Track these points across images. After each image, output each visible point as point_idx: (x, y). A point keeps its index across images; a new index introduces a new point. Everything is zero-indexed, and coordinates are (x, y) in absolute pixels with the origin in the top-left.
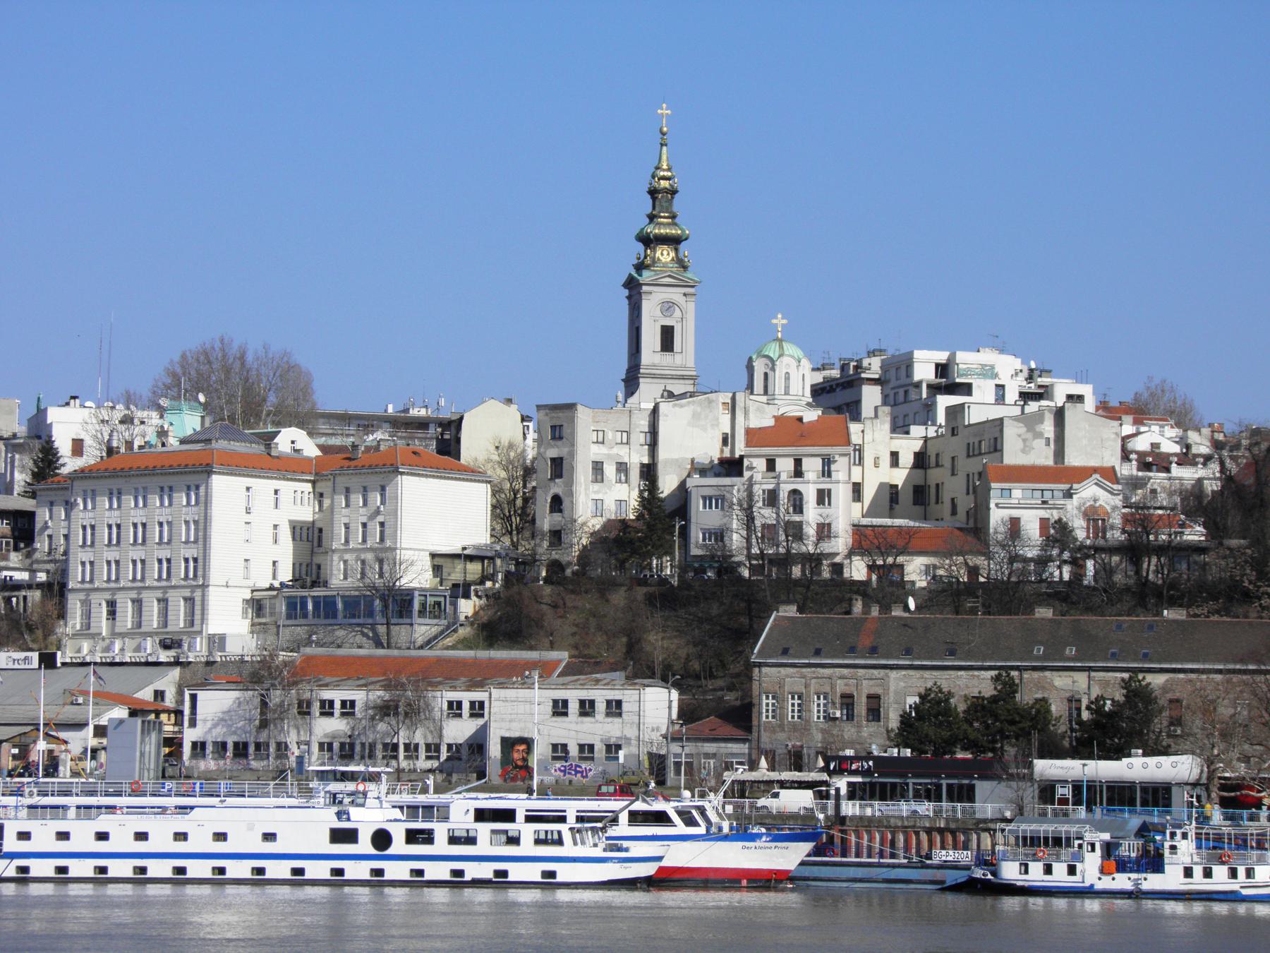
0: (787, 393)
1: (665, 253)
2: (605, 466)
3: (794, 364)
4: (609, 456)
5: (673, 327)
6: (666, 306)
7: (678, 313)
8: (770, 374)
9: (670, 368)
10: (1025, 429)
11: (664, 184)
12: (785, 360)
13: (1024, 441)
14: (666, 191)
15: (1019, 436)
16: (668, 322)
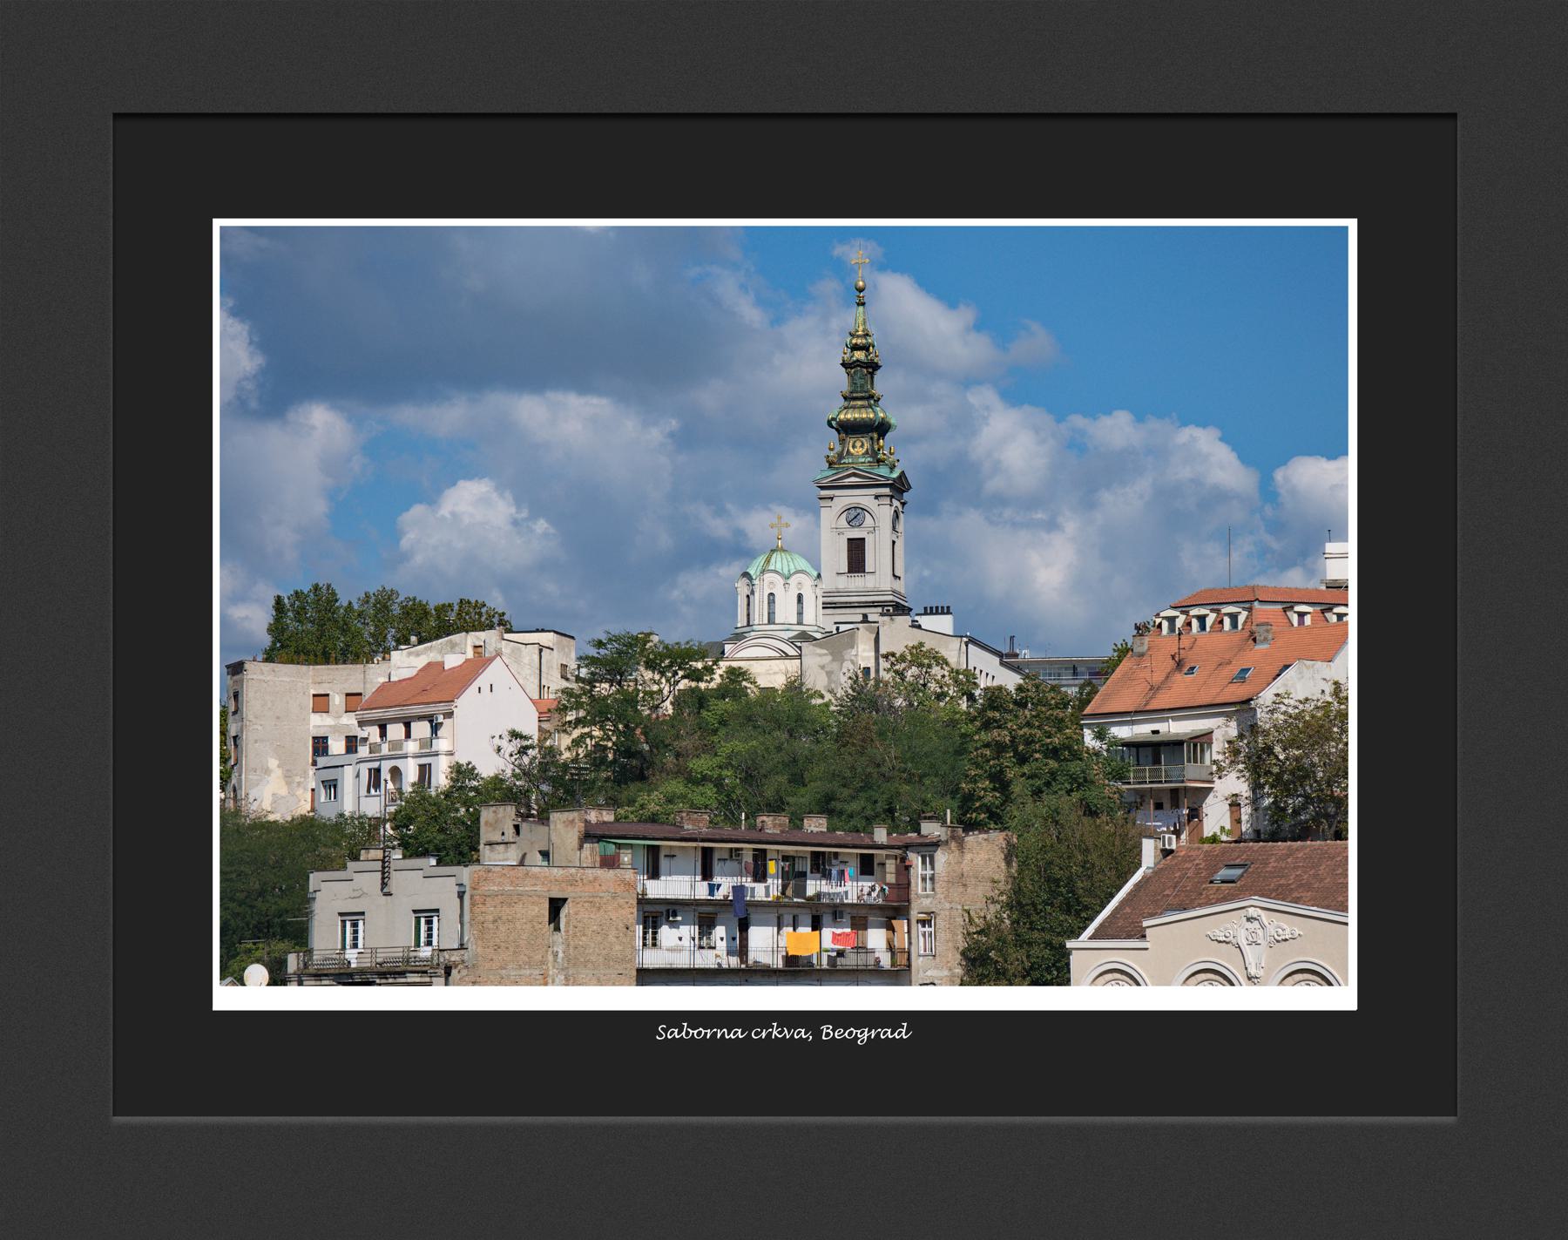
0: (771, 621)
1: (858, 444)
2: (330, 742)
3: (779, 580)
4: (335, 729)
5: (864, 539)
6: (853, 513)
7: (868, 521)
8: (751, 597)
9: (859, 593)
10: (829, 658)
11: (860, 355)
12: (768, 576)
13: (829, 674)
14: (858, 364)
15: (823, 667)
16: (856, 534)
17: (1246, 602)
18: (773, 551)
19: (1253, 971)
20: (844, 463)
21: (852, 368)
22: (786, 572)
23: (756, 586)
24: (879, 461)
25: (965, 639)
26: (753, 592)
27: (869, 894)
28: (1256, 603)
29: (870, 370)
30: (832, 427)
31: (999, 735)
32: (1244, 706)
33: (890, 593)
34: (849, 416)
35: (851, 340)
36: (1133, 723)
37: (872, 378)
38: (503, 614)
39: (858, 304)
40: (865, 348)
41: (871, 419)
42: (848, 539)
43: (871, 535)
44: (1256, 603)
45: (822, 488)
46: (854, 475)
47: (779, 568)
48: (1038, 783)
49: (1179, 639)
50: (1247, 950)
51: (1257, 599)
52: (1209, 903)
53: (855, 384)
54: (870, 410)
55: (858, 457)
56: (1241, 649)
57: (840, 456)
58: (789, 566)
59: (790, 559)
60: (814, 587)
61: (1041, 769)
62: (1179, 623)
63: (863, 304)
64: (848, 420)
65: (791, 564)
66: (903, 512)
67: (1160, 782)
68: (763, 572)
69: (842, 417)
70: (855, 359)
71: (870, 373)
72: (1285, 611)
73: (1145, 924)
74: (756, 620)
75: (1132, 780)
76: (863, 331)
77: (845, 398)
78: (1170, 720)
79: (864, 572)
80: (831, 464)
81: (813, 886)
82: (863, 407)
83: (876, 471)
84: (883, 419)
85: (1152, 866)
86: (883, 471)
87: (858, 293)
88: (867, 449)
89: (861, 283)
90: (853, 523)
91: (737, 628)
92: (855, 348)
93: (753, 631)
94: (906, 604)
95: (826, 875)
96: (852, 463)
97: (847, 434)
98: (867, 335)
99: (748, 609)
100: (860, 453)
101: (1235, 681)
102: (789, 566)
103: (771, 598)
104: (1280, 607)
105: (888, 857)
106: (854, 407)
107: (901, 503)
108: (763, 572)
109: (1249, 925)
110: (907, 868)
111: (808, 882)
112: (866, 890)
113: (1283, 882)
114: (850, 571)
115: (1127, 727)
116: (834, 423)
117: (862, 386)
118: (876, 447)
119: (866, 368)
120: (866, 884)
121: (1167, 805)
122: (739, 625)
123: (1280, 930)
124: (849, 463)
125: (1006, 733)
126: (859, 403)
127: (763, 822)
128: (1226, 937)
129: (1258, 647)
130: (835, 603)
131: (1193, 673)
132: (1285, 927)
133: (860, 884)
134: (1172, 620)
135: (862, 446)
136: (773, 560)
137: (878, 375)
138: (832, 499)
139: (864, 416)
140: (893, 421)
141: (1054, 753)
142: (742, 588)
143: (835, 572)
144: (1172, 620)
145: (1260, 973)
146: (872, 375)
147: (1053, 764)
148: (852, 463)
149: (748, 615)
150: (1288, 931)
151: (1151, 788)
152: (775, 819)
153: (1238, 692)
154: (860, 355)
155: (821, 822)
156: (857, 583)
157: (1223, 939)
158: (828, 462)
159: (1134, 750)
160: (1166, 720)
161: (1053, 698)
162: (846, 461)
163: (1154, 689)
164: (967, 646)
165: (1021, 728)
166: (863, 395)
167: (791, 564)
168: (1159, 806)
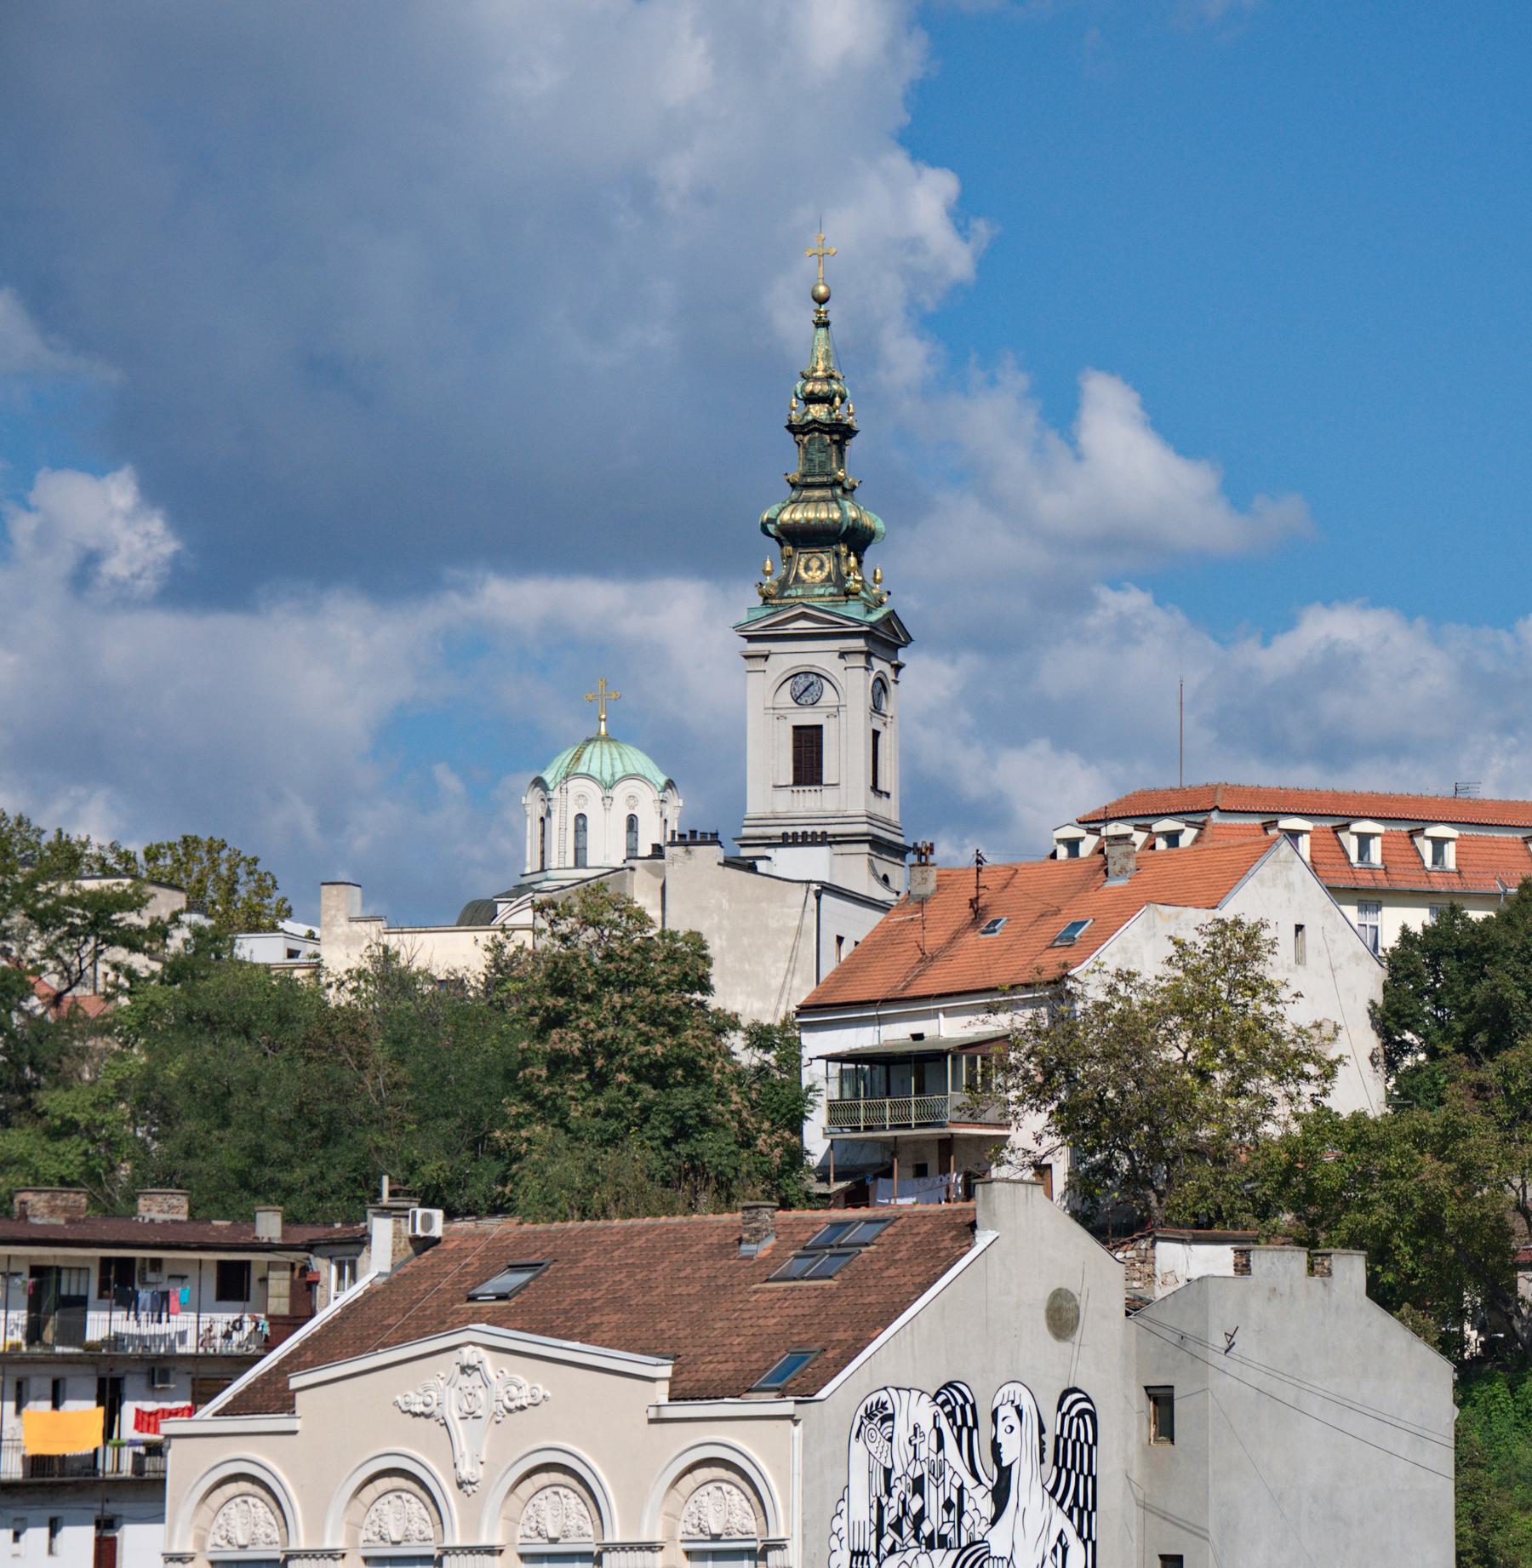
1: (815, 564)
3: (595, 791)
5: (820, 727)
6: (803, 682)
7: (829, 696)
8: (547, 821)
11: (818, 412)
12: (575, 785)
14: (813, 426)
16: (807, 718)
17: (1198, 812)
18: (589, 741)
19: (465, 1472)
20: (790, 597)
21: (805, 434)
22: (607, 777)
23: (553, 802)
24: (848, 593)
25: (815, 887)
26: (549, 813)
27: (227, 1336)
28: (1214, 815)
29: (836, 437)
30: (769, 535)
31: (562, 1039)
32: (1058, 989)
33: (865, 819)
34: (798, 516)
35: (803, 386)
36: (880, 1020)
37: (841, 452)
38: (255, 861)
39: (818, 325)
40: (827, 399)
41: (834, 522)
42: (796, 728)
43: (832, 720)
44: (1214, 815)
45: (751, 639)
46: (804, 616)
47: (594, 771)
48: (613, 1125)
49: (979, 870)
50: (458, 1428)
51: (1217, 807)
52: (403, 1339)
53: (811, 460)
54: (834, 505)
55: (814, 585)
56: (1084, 887)
57: (783, 584)
58: (613, 766)
59: (616, 755)
60: (658, 804)
61: (619, 1101)
62: (1085, 849)
63: (826, 325)
64: (796, 522)
65: (618, 763)
66: (896, 682)
67: (908, 1126)
68: (567, 777)
69: (786, 516)
70: (810, 418)
71: (835, 442)
72: (1335, 832)
73: (295, 1383)
74: (554, 861)
75: (913, 1122)
76: (825, 370)
77: (793, 485)
78: (941, 1015)
79: (819, 782)
80: (766, 598)
81: (100, 1325)
82: (824, 500)
83: (841, 611)
84: (855, 520)
85: (388, 1269)
86: (854, 610)
87: (816, 306)
88: (829, 573)
89: (822, 290)
90: (802, 701)
91: (523, 875)
92: (811, 399)
93: (547, 880)
94: (901, 840)
95: (127, 1301)
96: (803, 596)
97: (795, 546)
98: (832, 377)
99: (542, 842)
100: (817, 580)
101: (1057, 943)
102: (613, 766)
103: (581, 822)
104: (1257, 821)
105: (271, 1266)
106: (807, 501)
107: (892, 666)
108: (567, 777)
109: (464, 1380)
110: (311, 1286)
111: (91, 1315)
112: (219, 1329)
113: (587, 1295)
114: (798, 781)
115: (871, 1028)
116: (771, 528)
117: (822, 464)
118: (844, 569)
119: (829, 433)
120: (222, 1319)
121: (933, 1165)
122: (528, 870)
123: (513, 1390)
124: (797, 597)
125: (576, 1035)
126: (817, 493)
127: (23, 1203)
128: (426, 1405)
129: (1111, 884)
130: (769, 838)
131: (994, 931)
132: (522, 1381)
133: (205, 1317)
134: (1073, 845)
135: (821, 567)
136: (586, 757)
137: (853, 446)
138: (766, 657)
139: (824, 515)
140: (878, 524)
141: (656, 1073)
142: (532, 803)
143: (771, 783)
144: (1073, 845)
145: (479, 1473)
146: (840, 446)
147: (649, 1093)
148: (803, 596)
149: (543, 852)
150: (526, 1391)
151: (896, 1137)
152: (54, 1198)
153: (1050, 963)
154: (818, 412)
155: (174, 1202)
156: (808, 804)
157: (418, 1409)
158: (761, 594)
159: (880, 1070)
160: (933, 1014)
161: (664, 972)
162: (793, 593)
163: (927, 959)
164: (818, 898)
165: (600, 1026)
166: (825, 479)
167: (618, 763)
168: (921, 1171)
